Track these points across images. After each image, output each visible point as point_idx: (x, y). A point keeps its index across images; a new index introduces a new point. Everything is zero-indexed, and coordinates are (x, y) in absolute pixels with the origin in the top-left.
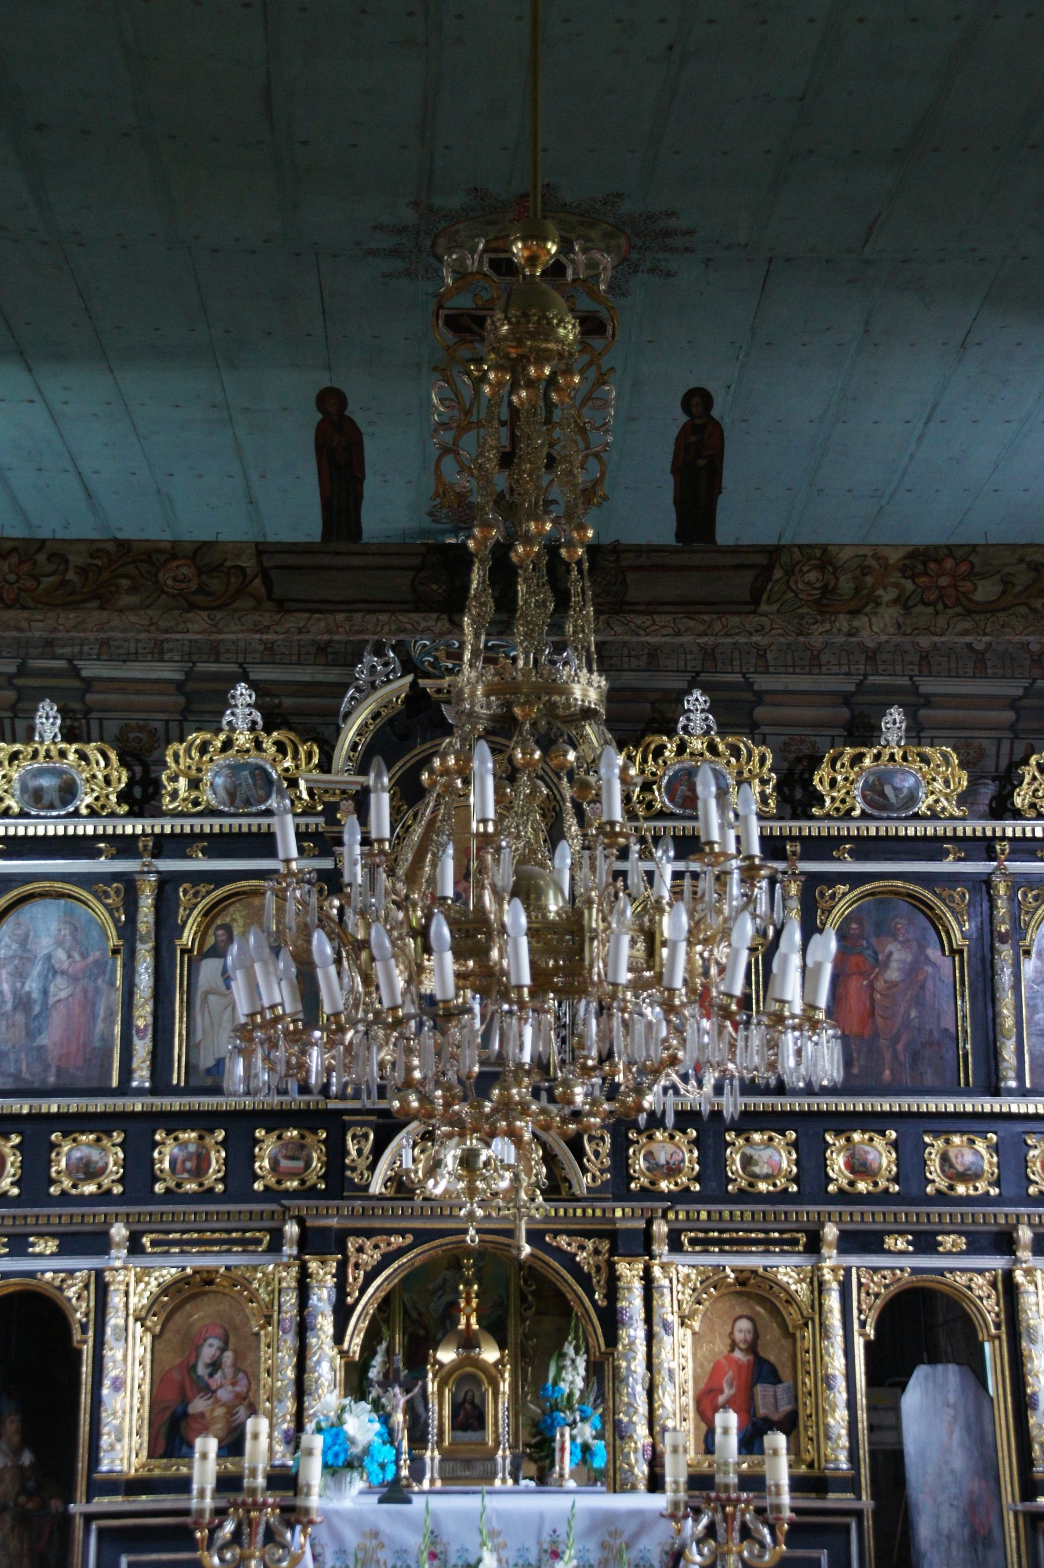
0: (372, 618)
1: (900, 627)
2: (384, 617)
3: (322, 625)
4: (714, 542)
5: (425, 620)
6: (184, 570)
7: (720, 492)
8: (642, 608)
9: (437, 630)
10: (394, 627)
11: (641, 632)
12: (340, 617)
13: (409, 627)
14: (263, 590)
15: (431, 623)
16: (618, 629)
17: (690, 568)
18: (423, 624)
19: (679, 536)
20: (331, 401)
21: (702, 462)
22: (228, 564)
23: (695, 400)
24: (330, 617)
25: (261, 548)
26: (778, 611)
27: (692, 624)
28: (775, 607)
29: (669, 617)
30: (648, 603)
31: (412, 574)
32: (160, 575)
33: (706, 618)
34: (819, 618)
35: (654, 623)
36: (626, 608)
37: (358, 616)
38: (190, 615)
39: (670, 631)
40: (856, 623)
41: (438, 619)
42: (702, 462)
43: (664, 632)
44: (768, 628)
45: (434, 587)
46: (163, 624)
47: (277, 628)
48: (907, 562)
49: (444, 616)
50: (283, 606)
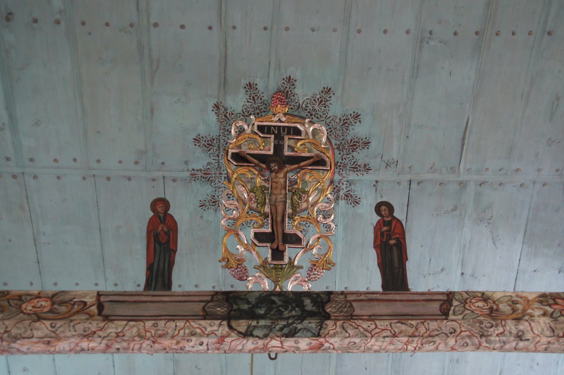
0: (172, 324)
1: (553, 331)
2: (181, 324)
3: (135, 330)
4: (407, 289)
5: (211, 326)
6: (43, 303)
7: (407, 260)
8: (366, 317)
9: (219, 333)
10: (187, 331)
11: (369, 335)
12: (149, 324)
13: (198, 331)
14: (96, 311)
15: (215, 328)
16: (351, 332)
17: (396, 301)
18: (209, 329)
19: (384, 286)
20: (161, 207)
21: (392, 242)
22: (75, 300)
23: (383, 208)
24: (142, 324)
25: (100, 293)
26: (463, 318)
27: (404, 327)
28: (460, 317)
29: (387, 323)
30: (370, 316)
31: (203, 304)
32: (24, 306)
33: (414, 323)
34: (494, 323)
35: (376, 327)
36: (354, 317)
37: (161, 323)
38: (38, 324)
39: (388, 333)
40: (521, 327)
41: (220, 325)
42: (392, 242)
43: (384, 334)
44: (458, 330)
45: (219, 309)
46: (14, 332)
47: (101, 333)
48: (541, 299)
49: (225, 323)
50: (107, 318)
